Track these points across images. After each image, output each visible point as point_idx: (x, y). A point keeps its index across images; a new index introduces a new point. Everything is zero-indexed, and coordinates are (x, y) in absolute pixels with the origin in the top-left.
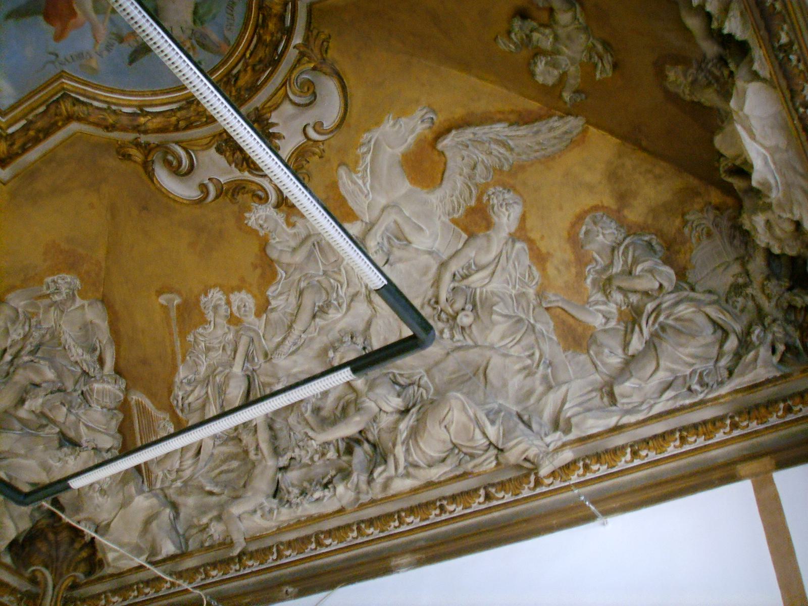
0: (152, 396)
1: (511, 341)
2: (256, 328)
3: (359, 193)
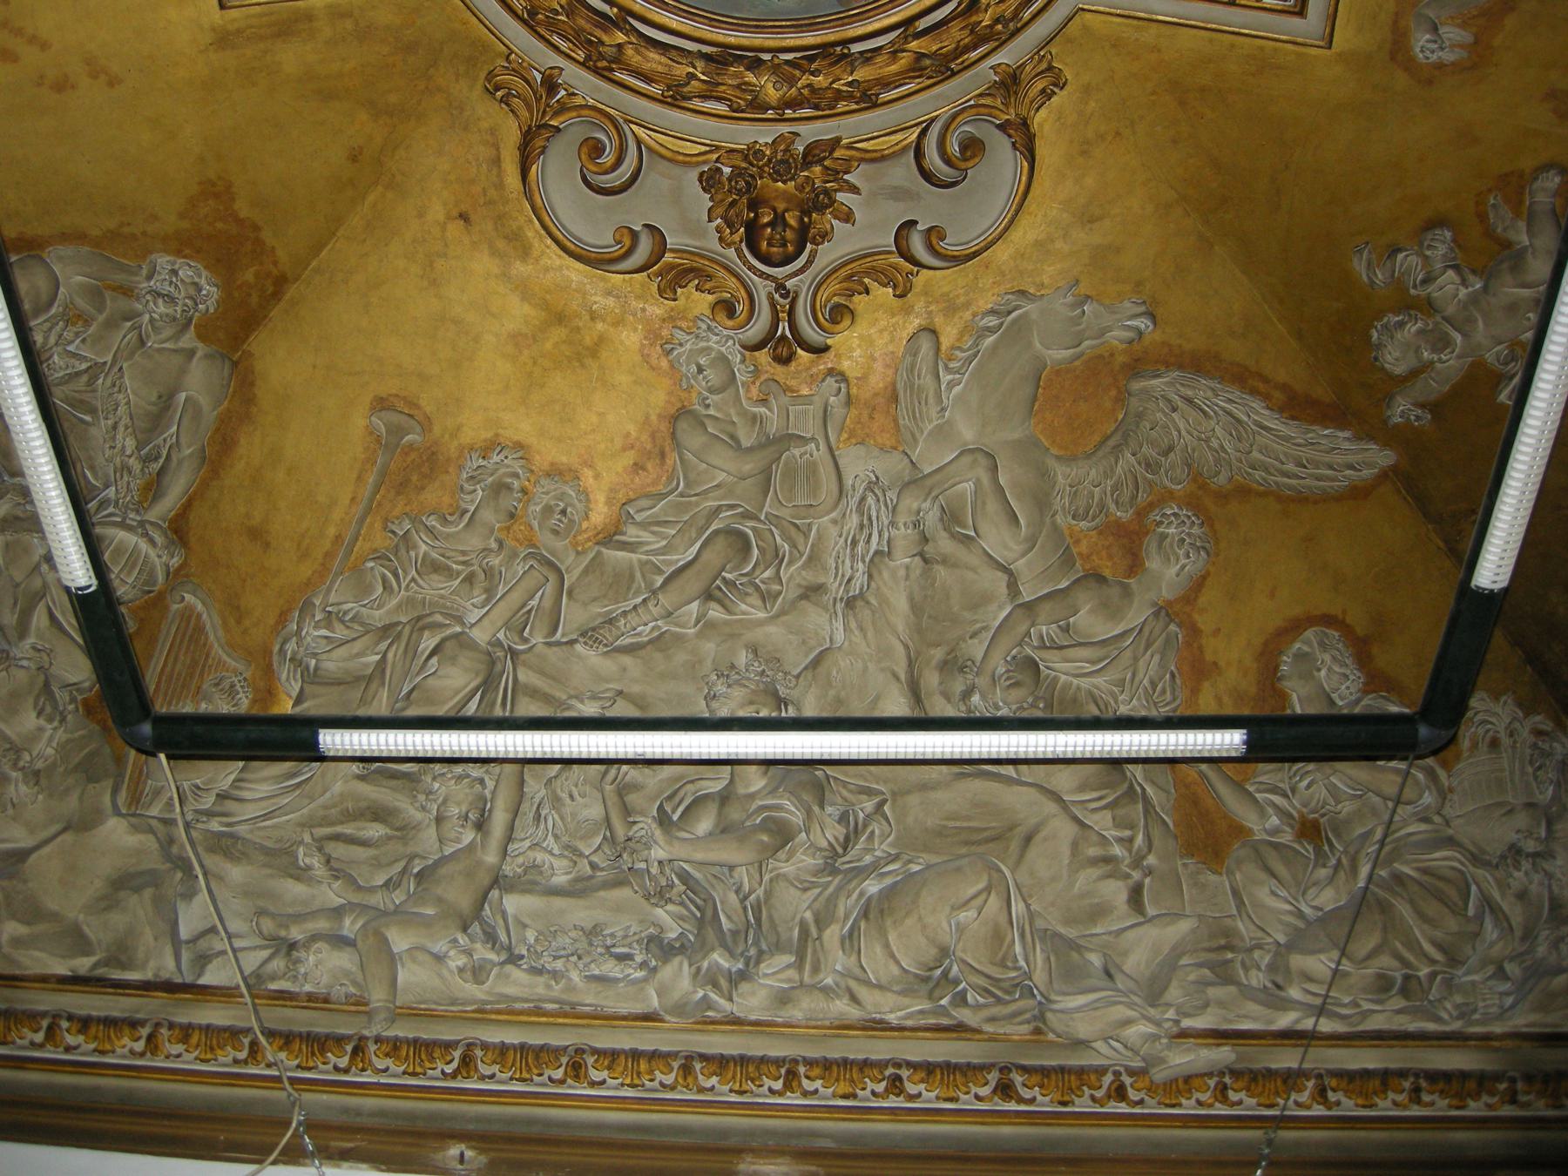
0: (234, 609)
1: (1100, 798)
2: (563, 569)
3: (931, 401)
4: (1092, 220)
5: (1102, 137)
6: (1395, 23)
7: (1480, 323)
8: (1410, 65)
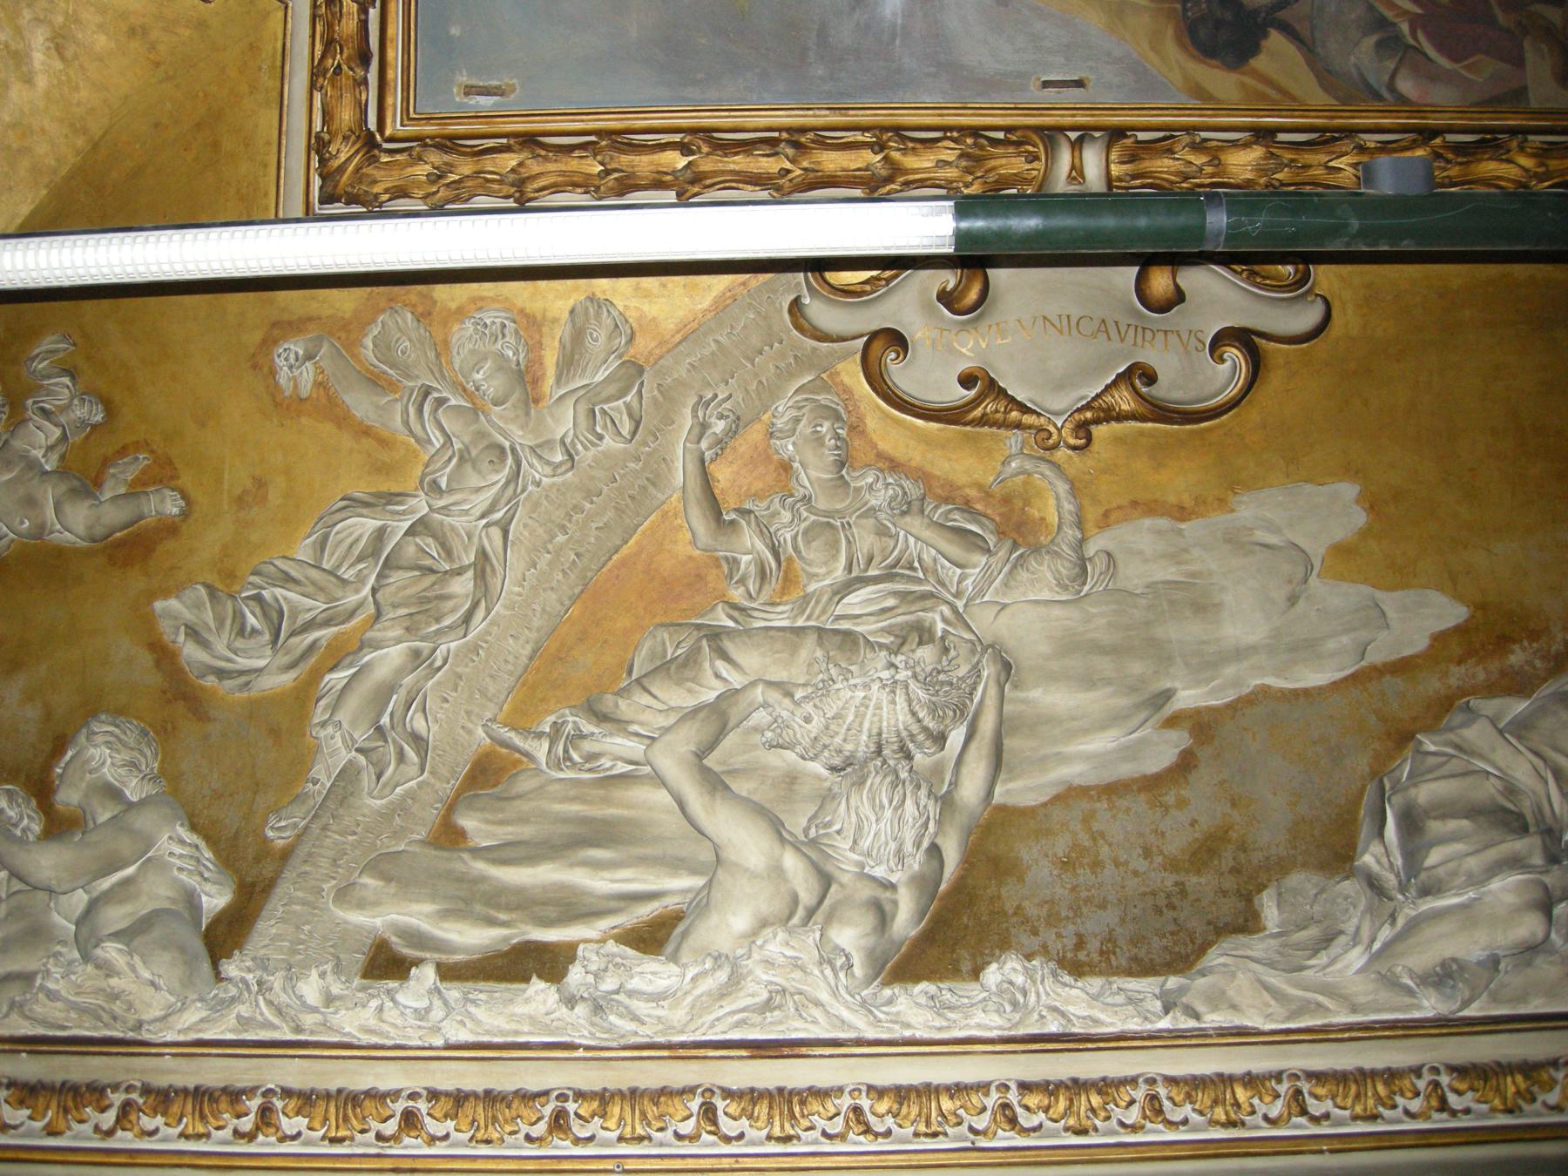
4: (59, 50)
5: (153, 47)
6: (310, 319)
7: (7, 477)
8: (269, 343)
